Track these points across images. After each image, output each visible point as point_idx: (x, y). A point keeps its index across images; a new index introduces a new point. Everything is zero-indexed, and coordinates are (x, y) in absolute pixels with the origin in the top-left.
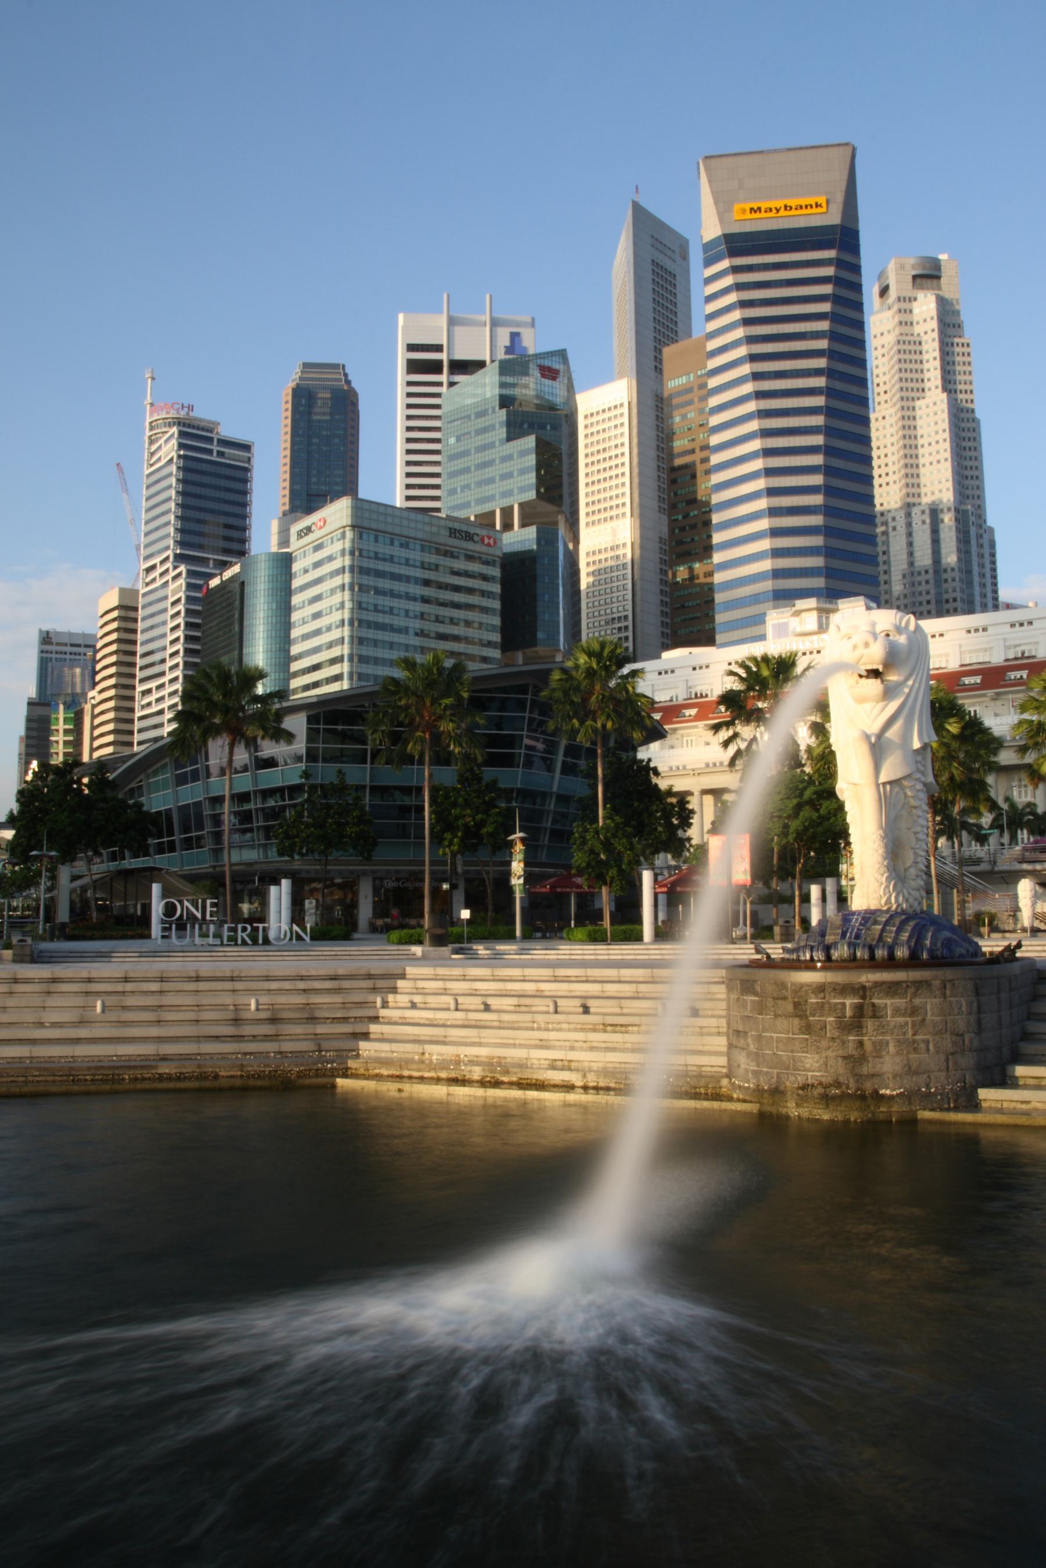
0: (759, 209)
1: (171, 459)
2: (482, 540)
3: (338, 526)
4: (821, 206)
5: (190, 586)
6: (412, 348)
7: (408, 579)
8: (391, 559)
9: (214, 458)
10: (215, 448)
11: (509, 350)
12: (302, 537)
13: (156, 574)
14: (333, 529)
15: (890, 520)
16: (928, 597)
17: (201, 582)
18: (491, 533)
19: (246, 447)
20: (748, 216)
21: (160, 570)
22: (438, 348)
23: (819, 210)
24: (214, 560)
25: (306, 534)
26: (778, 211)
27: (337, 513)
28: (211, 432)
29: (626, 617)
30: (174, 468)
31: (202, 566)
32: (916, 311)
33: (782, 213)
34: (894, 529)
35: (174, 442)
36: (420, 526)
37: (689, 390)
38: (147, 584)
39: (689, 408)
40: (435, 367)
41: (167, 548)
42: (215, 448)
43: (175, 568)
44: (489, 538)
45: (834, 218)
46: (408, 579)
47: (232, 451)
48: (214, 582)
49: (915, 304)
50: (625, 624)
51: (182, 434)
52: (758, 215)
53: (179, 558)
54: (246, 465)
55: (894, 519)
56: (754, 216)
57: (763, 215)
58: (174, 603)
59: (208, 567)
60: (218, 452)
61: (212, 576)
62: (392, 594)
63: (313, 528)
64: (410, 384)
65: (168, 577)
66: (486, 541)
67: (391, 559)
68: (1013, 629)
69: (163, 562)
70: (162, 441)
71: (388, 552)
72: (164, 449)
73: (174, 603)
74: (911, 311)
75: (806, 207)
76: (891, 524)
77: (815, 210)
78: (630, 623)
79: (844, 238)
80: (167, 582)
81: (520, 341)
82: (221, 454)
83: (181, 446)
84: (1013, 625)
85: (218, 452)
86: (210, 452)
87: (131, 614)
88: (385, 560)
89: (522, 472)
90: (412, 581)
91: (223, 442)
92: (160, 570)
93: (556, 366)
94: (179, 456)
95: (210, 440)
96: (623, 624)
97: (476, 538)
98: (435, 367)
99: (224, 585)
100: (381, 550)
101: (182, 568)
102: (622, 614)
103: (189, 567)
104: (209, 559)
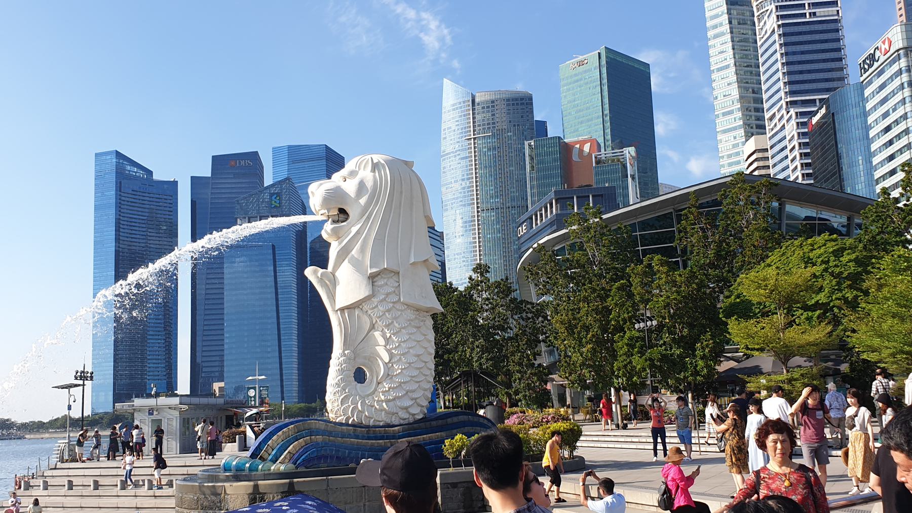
9: (808, 19)
10: (807, 11)
17: (806, 120)
21: (778, 117)
24: (820, 100)
30: (776, 36)
31: (810, 106)
35: (774, 16)
43: (788, 112)
48: (815, 120)
54: (836, 17)
60: (810, 14)
61: (814, 114)
65: (784, 121)
69: (778, 111)
70: (766, 18)
80: (784, 125)
83: (779, 17)
87: (766, 154)
92: (778, 117)
94: (779, 26)
101: (792, 112)
104: (815, 100)
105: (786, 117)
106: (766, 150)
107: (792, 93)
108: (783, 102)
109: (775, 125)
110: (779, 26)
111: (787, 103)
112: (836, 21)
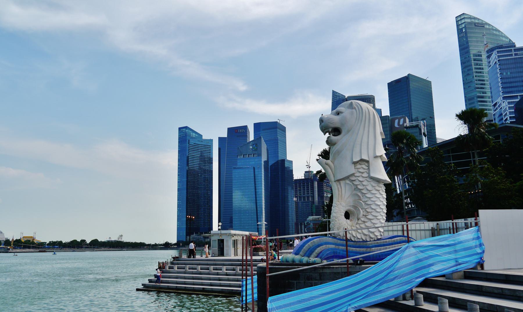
1: (496, 62)
5: (510, 108)
38: (495, 111)
41: (500, 96)
51: (498, 52)
53: (504, 98)
58: (505, 116)
59: (518, 98)
73: (505, 116)
83: (499, 56)
86: (511, 55)
91: (515, 50)
94: (499, 61)
95: (511, 51)
106: (492, 121)
110: (499, 61)
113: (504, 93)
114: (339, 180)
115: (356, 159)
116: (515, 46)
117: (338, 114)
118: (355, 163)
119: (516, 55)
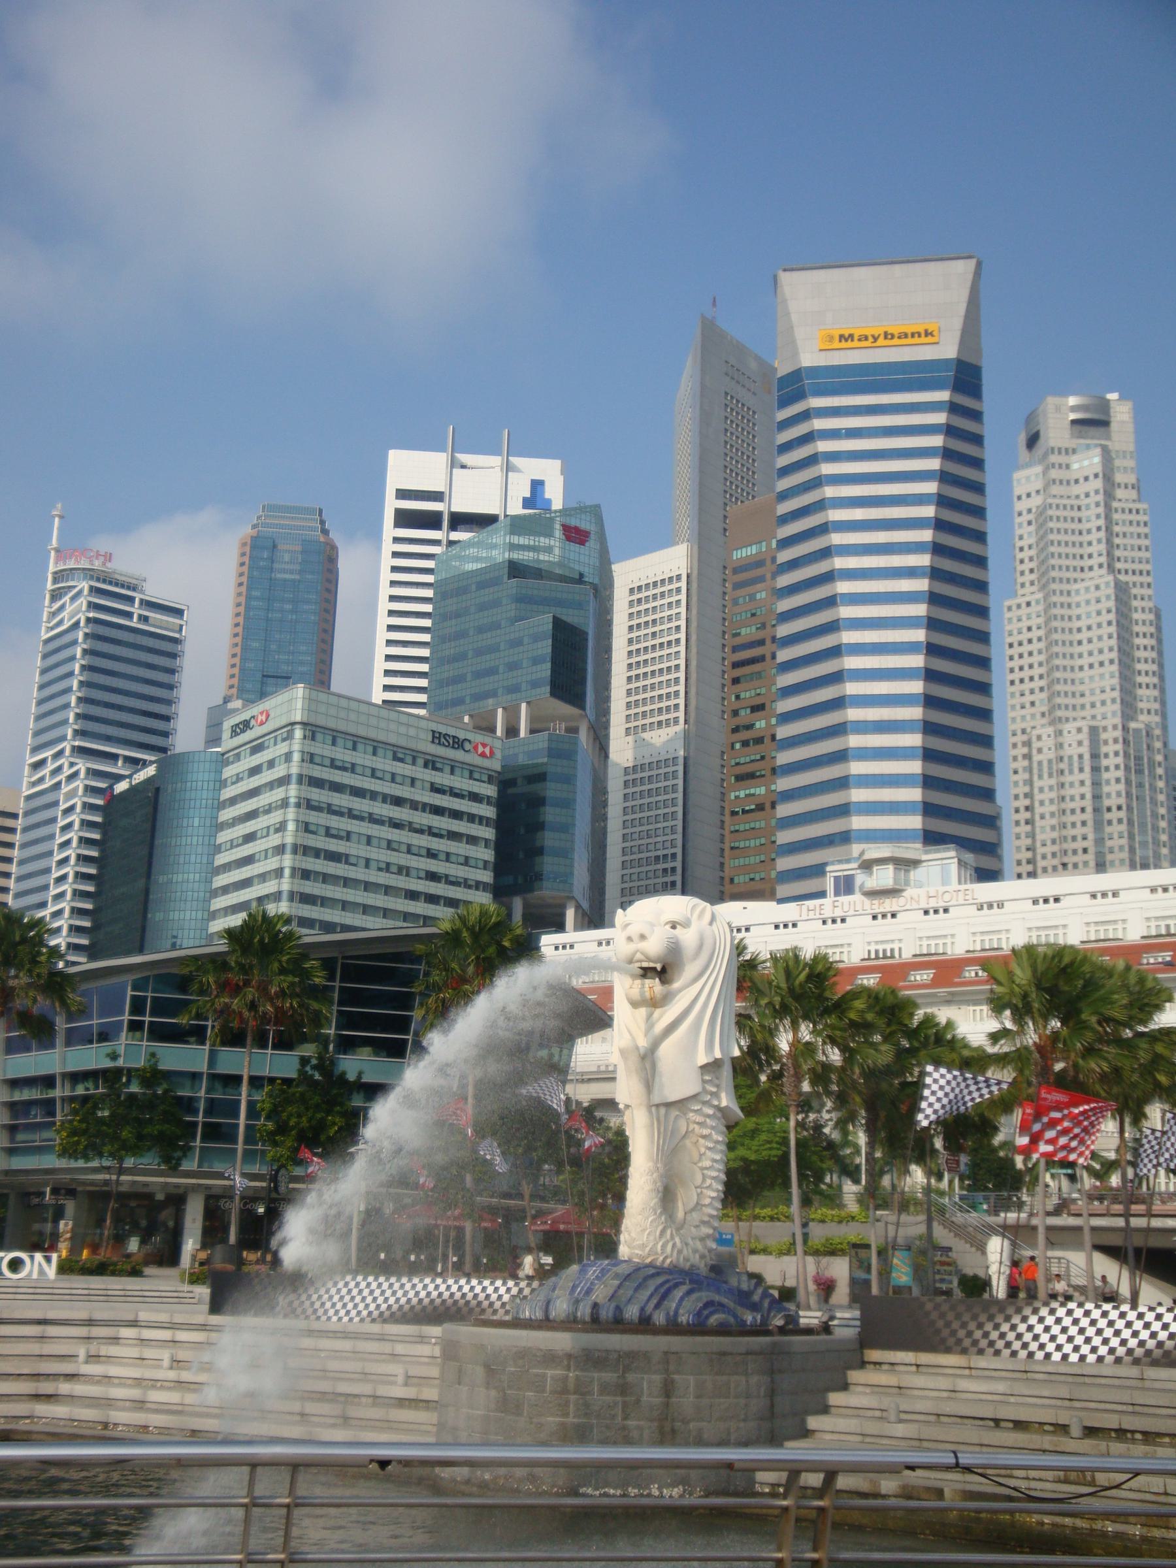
0: (851, 336)
2: (476, 748)
3: (284, 722)
4: (931, 334)
5: (90, 790)
6: (402, 494)
7: (373, 795)
8: (353, 768)
9: (134, 623)
10: (136, 610)
11: (527, 503)
12: (237, 734)
13: (46, 771)
14: (277, 725)
15: (1034, 739)
16: (1085, 844)
18: (488, 740)
19: (178, 612)
20: (837, 345)
21: (51, 766)
22: (437, 496)
23: (929, 339)
24: (128, 760)
25: (243, 731)
26: (875, 339)
27: (291, 703)
28: (134, 589)
29: (674, 856)
32: (1075, 466)
33: (879, 343)
34: (1040, 751)
35: (83, 602)
36: (393, 726)
37: (759, 563)
38: (34, 784)
39: (759, 586)
40: (431, 521)
41: (63, 738)
42: (136, 610)
43: (72, 765)
44: (484, 745)
45: (948, 349)
46: (373, 795)
47: (159, 616)
48: (121, 787)
49: (1074, 458)
50: (673, 865)
51: (95, 591)
52: (849, 344)
54: (177, 635)
55: (1039, 738)
56: (844, 344)
57: (856, 344)
60: (140, 616)
61: (119, 778)
62: (351, 814)
63: (253, 722)
64: (396, 540)
65: (62, 777)
66: (480, 749)
67: (353, 768)
68: (1154, 896)
70: (67, 598)
71: (347, 758)
72: (69, 608)
74: (1068, 467)
75: (913, 335)
76: (1036, 745)
77: (923, 340)
78: (678, 864)
79: (965, 378)
80: (59, 784)
81: (543, 492)
82: (145, 619)
84: (1153, 890)
85: (140, 616)
86: (129, 615)
88: (344, 769)
89: (536, 661)
90: (380, 798)
92: (51, 766)
93: (584, 526)
94: (88, 620)
95: (131, 600)
96: (669, 865)
97: (467, 746)
98: (431, 521)
99: (133, 790)
100: (339, 756)
101: (82, 766)
102: (669, 851)
103: (90, 765)
105: (67, 771)
106: (14, 816)
107: (78, 733)
108: (67, 746)
109: (41, 780)
110: (88, 620)
111: (73, 747)
112: (176, 641)
113: (78, 733)
114: (657, 1106)
115: (711, 1060)
116: (142, 592)
117: (674, 927)
118: (702, 1067)
119: (145, 619)
